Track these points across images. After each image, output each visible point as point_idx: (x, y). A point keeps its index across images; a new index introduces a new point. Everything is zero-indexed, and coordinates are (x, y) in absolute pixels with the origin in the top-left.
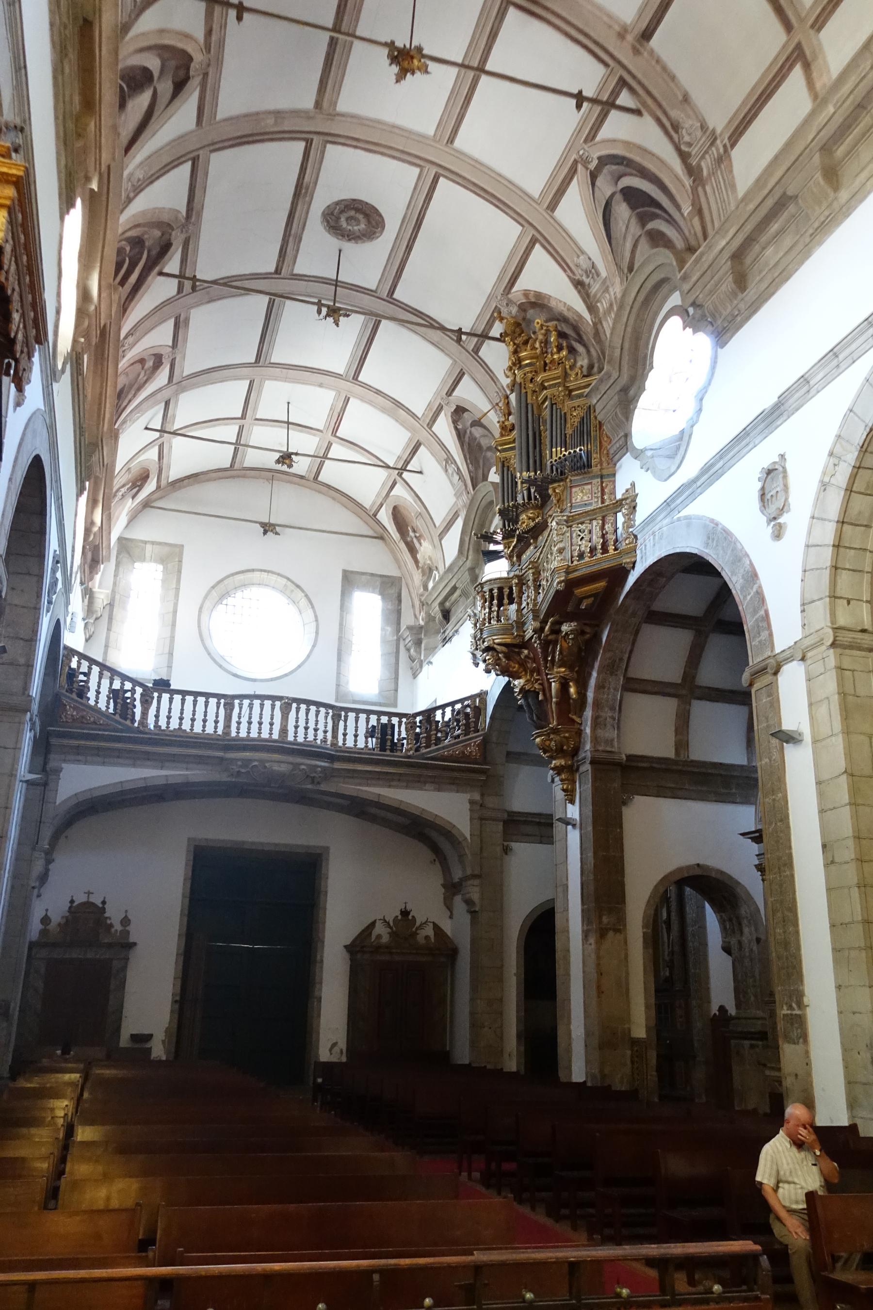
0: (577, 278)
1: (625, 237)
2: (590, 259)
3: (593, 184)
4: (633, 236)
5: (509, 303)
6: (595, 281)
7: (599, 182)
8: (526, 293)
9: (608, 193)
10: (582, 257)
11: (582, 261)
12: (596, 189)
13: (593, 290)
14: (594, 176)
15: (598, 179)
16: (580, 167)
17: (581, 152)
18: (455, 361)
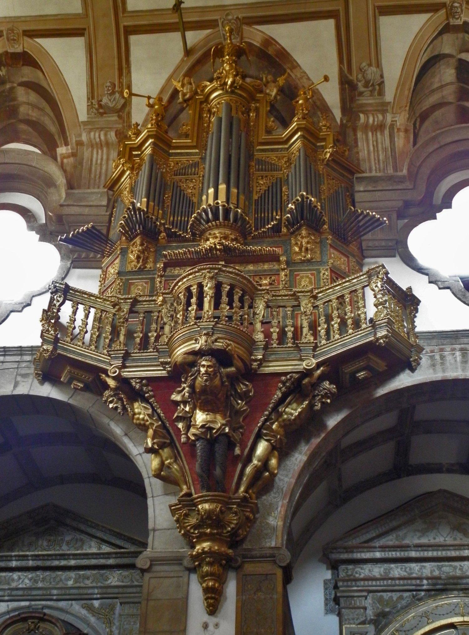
0: (351, 78)
1: (433, 91)
2: (382, 76)
3: (440, 33)
4: (443, 97)
5: (239, 32)
6: (371, 95)
7: (445, 37)
8: (269, 41)
9: (447, 50)
10: (374, 69)
11: (371, 73)
12: (440, 38)
13: (363, 100)
14: (447, 29)
15: (448, 34)
16: (444, 11)
17: (456, 5)
18: (87, 15)
